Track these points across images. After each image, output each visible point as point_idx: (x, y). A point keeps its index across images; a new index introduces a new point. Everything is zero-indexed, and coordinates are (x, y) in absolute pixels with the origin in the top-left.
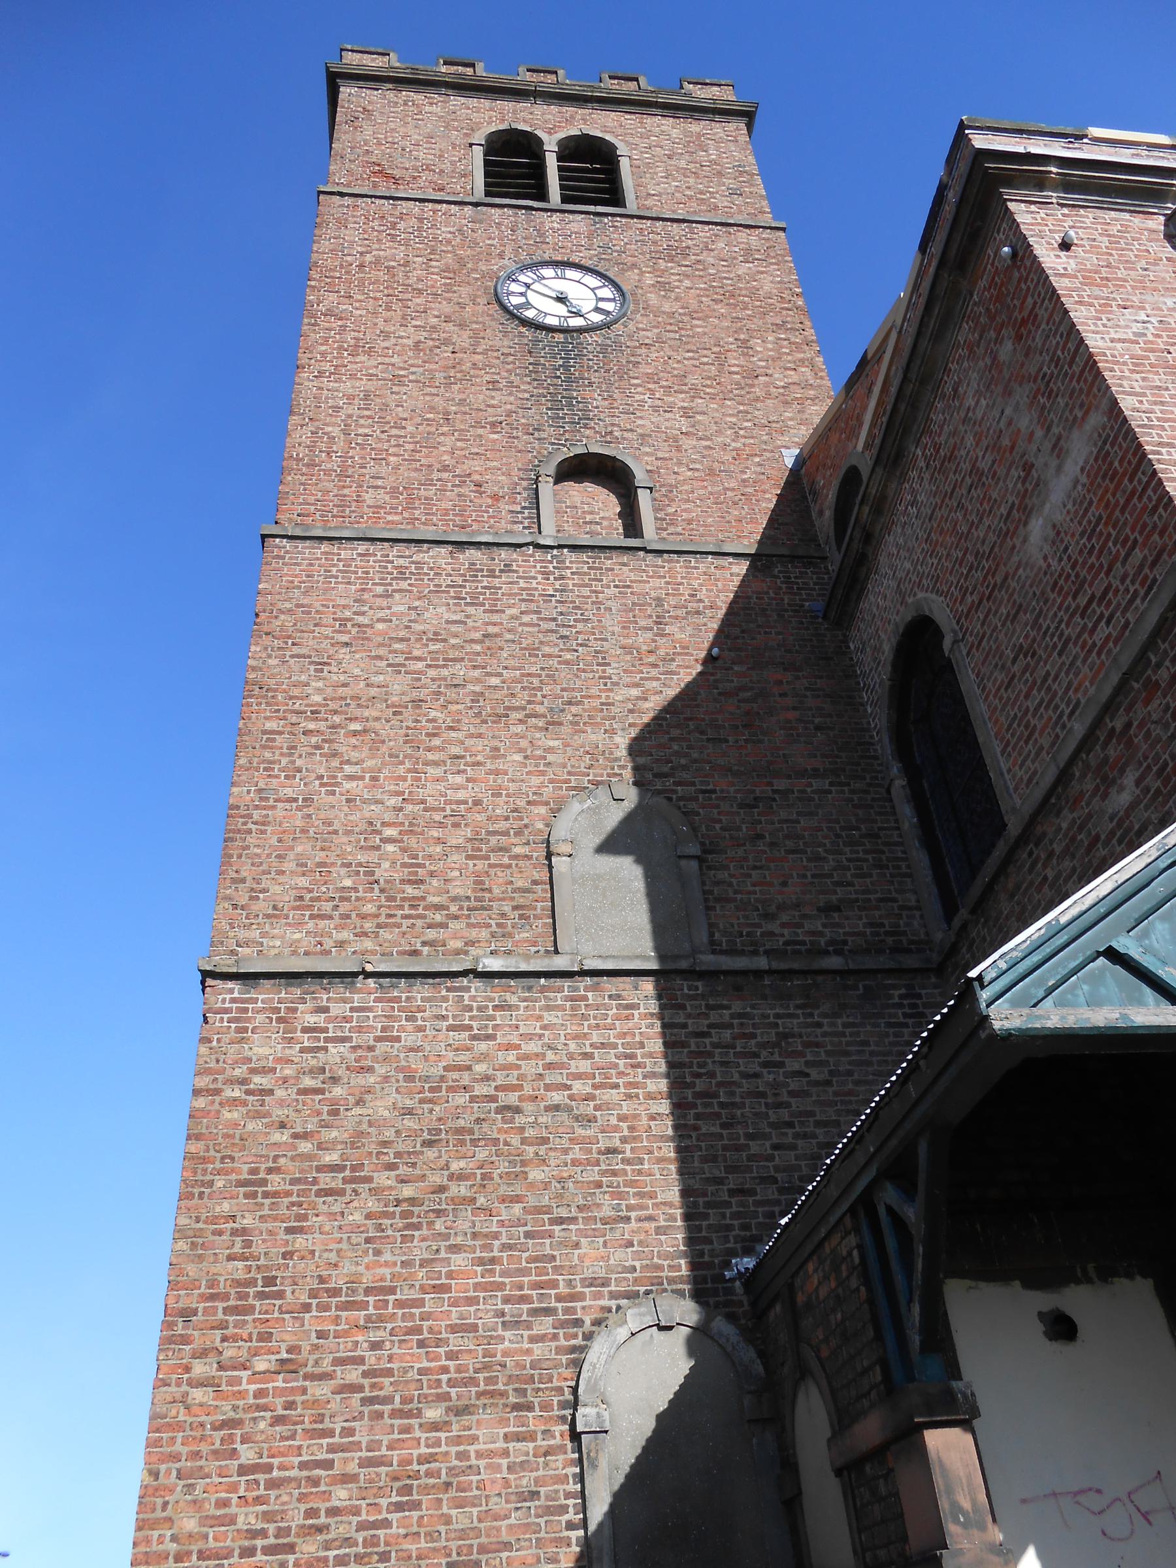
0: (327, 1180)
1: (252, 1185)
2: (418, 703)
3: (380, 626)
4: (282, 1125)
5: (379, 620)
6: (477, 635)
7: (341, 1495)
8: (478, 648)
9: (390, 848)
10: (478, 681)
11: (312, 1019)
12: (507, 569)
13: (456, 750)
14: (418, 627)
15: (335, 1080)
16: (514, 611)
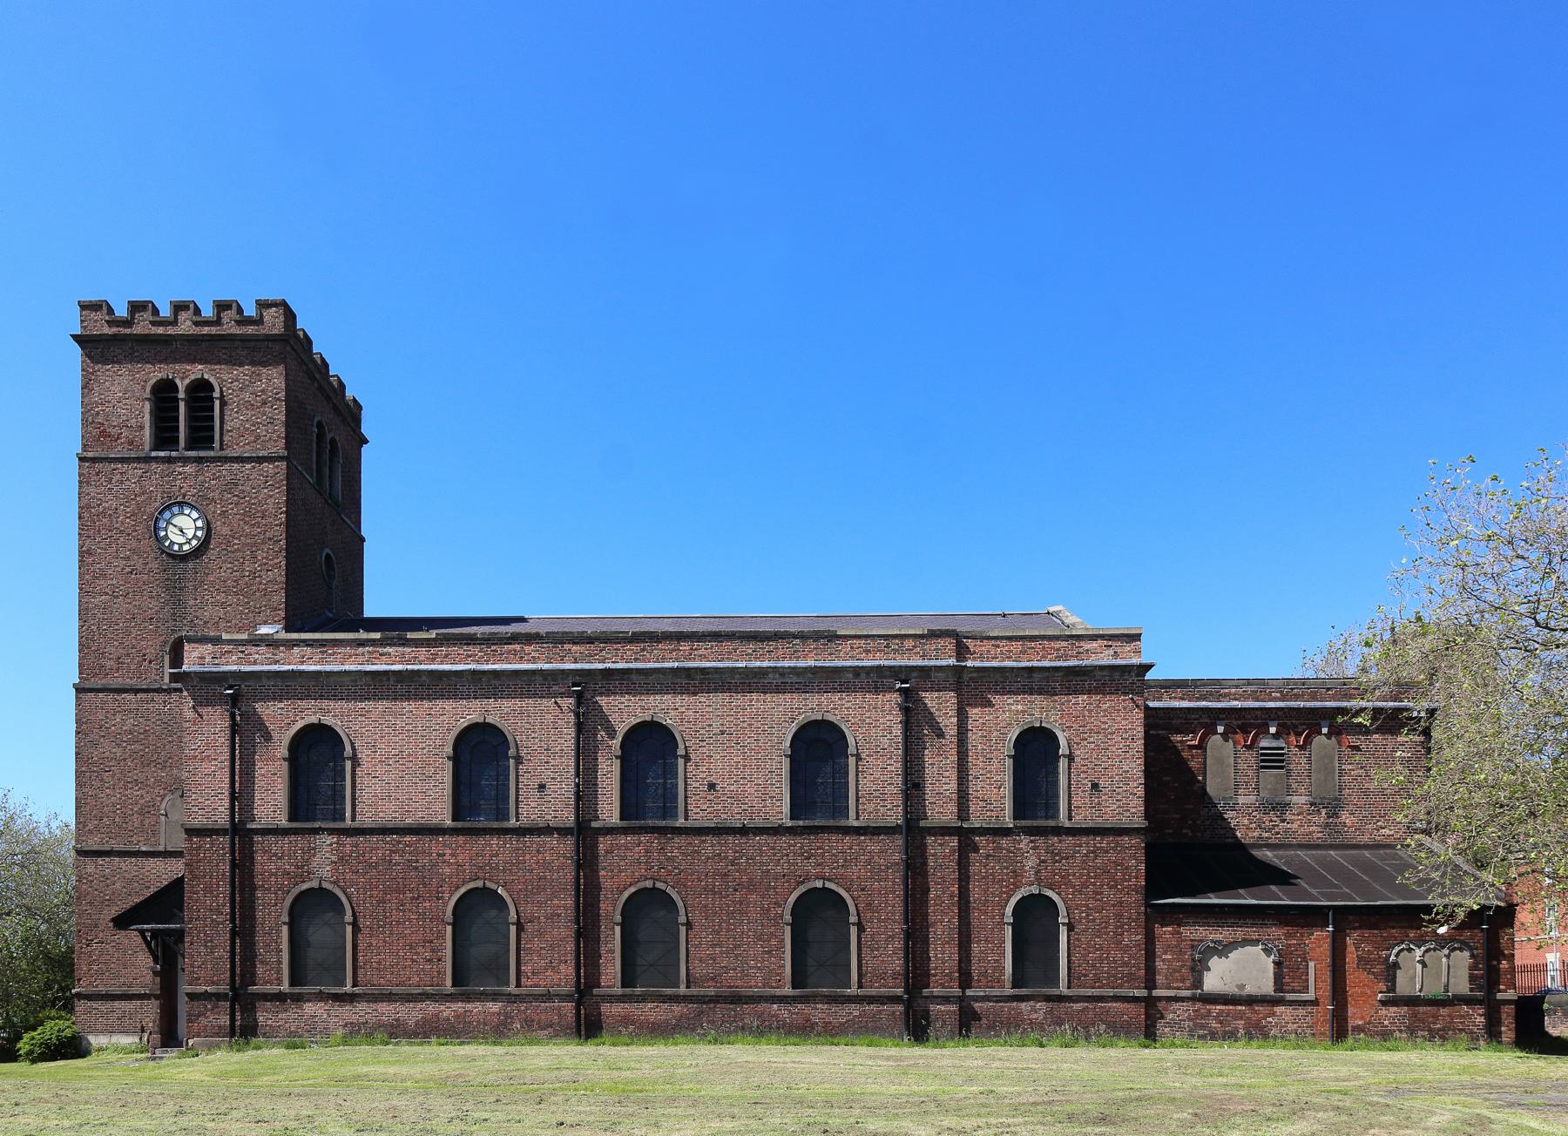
0: (106, 903)
1: (91, 903)
2: (125, 760)
3: (113, 728)
4: (96, 890)
5: (114, 725)
6: (142, 731)
7: (112, 965)
8: (142, 736)
9: (118, 812)
10: (141, 750)
11: (101, 862)
12: (153, 700)
13: (135, 778)
14: (124, 728)
15: (107, 879)
16: (153, 720)
